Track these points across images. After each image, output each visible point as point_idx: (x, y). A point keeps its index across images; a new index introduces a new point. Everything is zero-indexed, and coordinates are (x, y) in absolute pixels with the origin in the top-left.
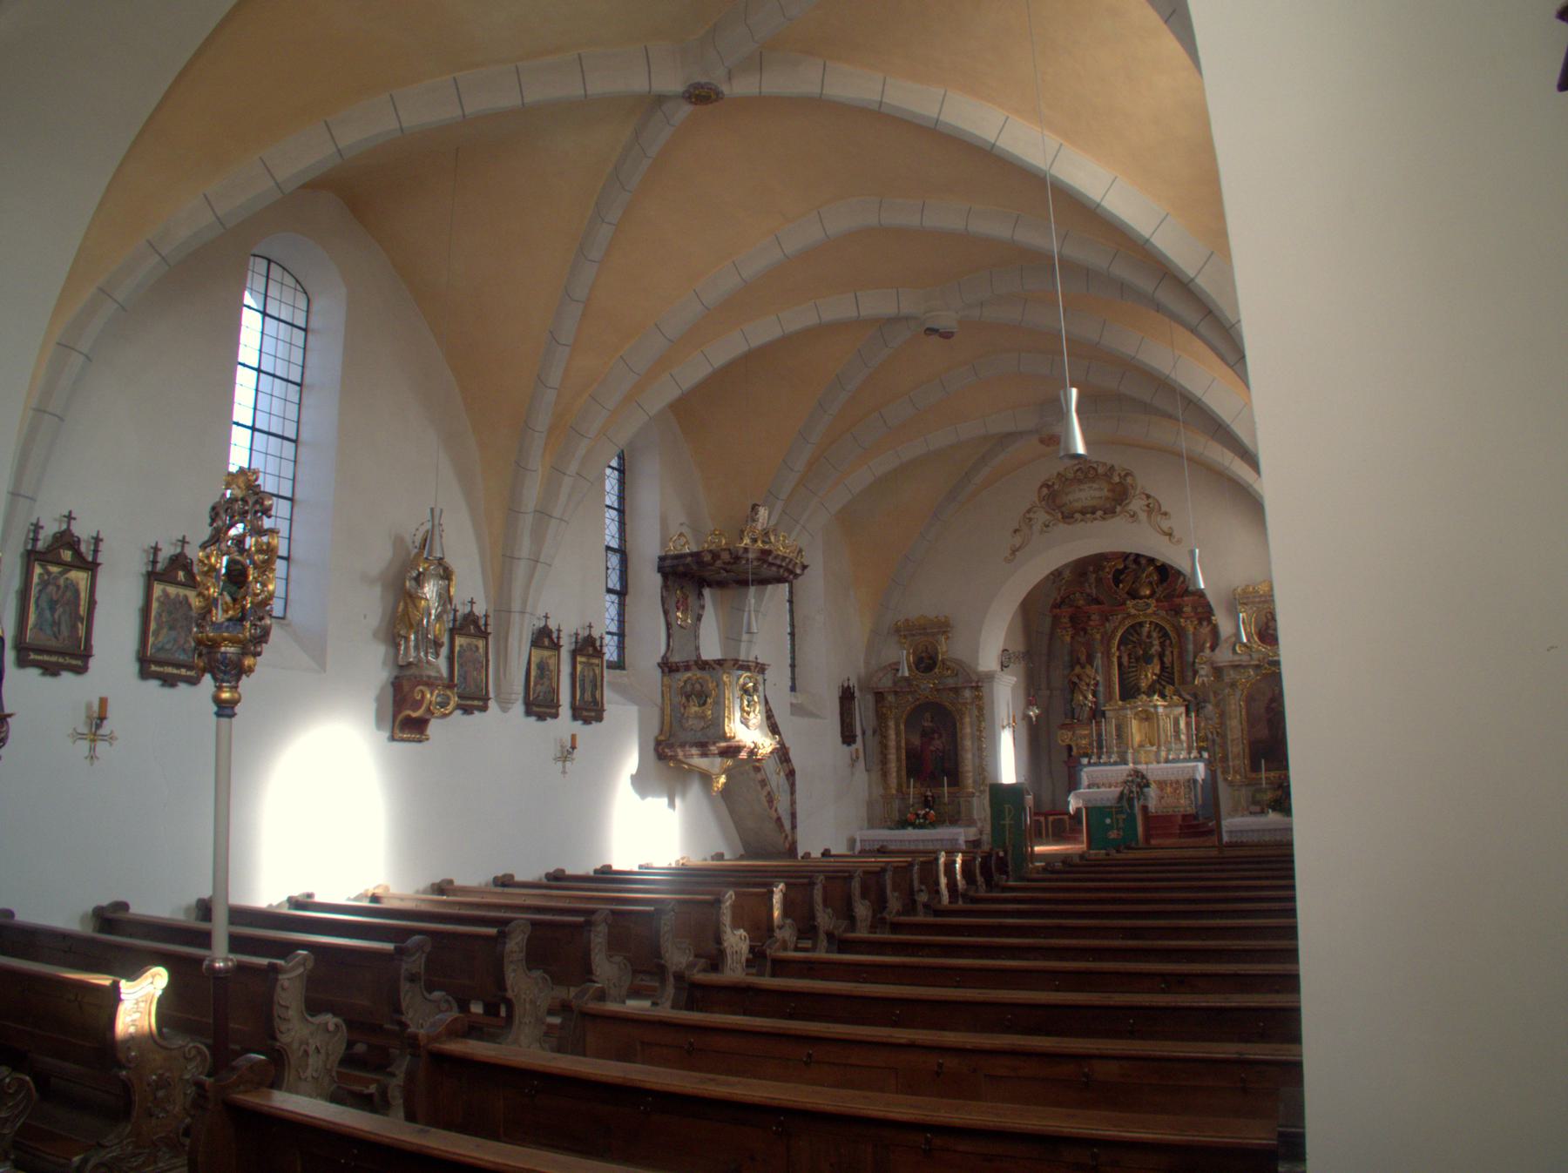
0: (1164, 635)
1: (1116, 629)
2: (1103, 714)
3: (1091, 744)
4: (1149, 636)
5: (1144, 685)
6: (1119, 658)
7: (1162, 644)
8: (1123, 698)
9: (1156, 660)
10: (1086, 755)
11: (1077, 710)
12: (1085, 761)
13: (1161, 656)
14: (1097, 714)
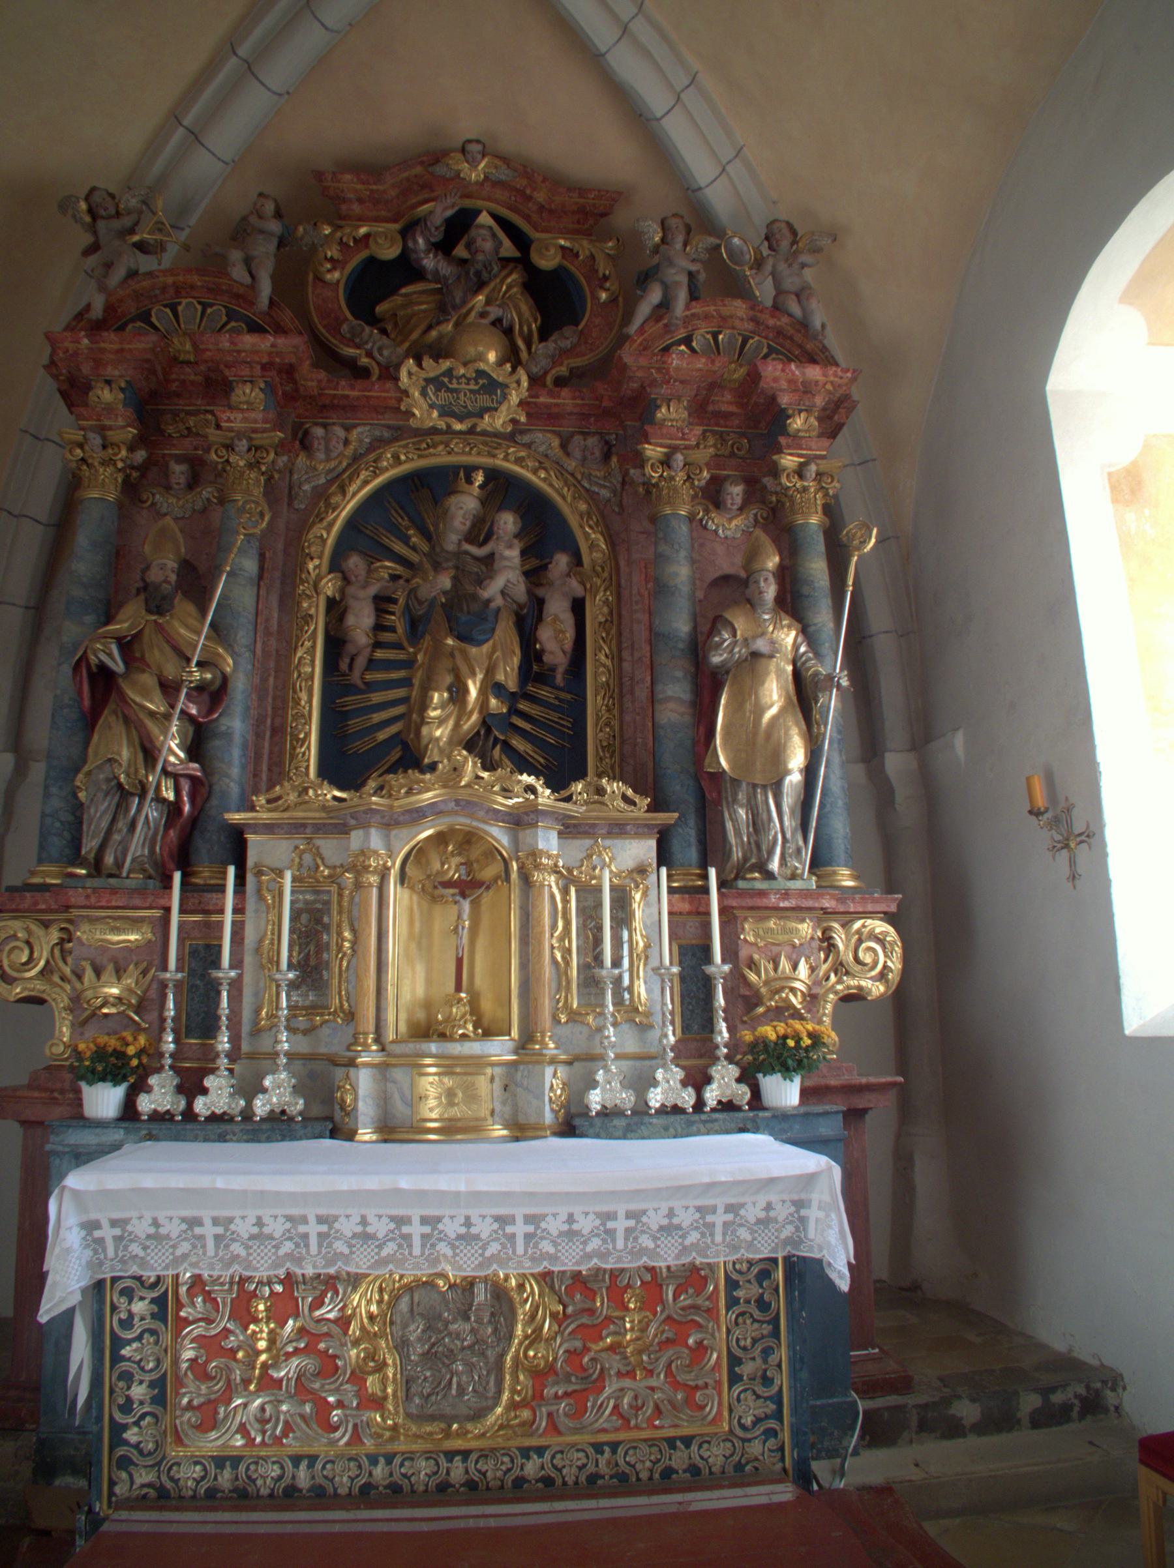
0: (544, 532)
1: (340, 482)
2: (236, 846)
3: (146, 1004)
4: (481, 531)
5: (439, 729)
6: (336, 609)
7: (535, 575)
8: (343, 766)
9: (505, 632)
10: (111, 1066)
11: (99, 814)
12: (104, 1100)
13: (528, 621)
14: (201, 846)
